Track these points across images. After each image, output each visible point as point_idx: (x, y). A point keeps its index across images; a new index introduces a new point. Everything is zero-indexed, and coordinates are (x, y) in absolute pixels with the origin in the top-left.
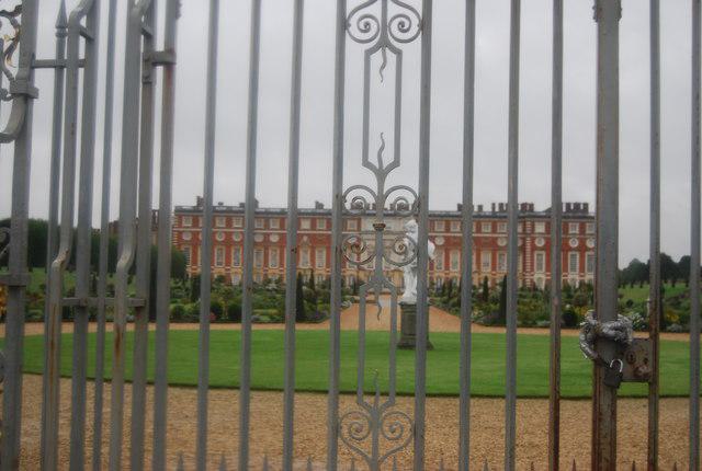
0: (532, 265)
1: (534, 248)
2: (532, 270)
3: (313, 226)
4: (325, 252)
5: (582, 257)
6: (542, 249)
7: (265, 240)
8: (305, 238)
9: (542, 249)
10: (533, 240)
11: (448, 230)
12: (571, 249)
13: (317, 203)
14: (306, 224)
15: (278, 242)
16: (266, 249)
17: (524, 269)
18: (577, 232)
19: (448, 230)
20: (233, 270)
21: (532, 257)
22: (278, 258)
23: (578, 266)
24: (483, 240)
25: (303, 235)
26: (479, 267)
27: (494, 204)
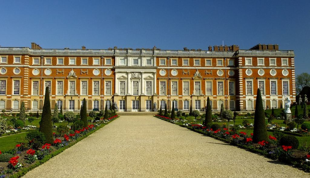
2: (244, 93)
3: (78, 63)
5: (280, 83)
7: (40, 74)
8: (72, 72)
10: (244, 70)
12: (272, 77)
14: (71, 62)
15: (52, 74)
19: (180, 65)
20: (13, 98)
21: (244, 83)
23: (277, 90)
24: (207, 72)
25: (71, 69)
26: (204, 93)
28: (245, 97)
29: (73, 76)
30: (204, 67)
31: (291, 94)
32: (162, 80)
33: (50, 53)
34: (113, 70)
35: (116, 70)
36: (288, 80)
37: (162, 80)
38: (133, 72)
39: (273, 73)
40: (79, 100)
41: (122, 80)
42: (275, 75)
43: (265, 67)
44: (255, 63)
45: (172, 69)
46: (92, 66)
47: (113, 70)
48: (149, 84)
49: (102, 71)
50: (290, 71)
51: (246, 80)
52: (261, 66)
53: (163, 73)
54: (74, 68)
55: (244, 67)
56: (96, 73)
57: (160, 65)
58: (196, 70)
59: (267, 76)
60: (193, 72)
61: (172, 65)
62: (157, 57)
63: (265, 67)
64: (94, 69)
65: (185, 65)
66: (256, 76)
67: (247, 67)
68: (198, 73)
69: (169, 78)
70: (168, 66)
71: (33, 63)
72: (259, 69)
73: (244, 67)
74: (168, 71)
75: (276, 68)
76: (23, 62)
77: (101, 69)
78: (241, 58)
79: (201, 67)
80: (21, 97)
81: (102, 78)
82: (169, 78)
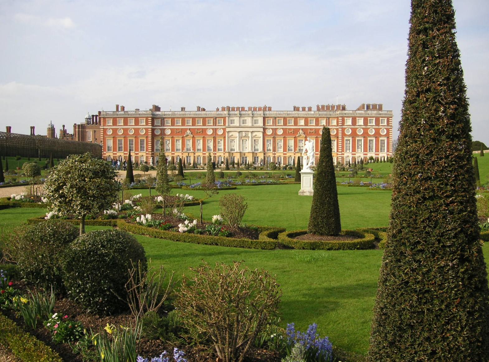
0: (343, 147)
1: (344, 134)
2: (343, 151)
4: (201, 141)
5: (377, 141)
6: (349, 136)
9: (349, 136)
10: (343, 130)
11: (285, 124)
12: (370, 136)
13: (199, 108)
16: (163, 139)
17: (337, 151)
18: (374, 124)
22: (170, 145)
25: (187, 129)
27: (318, 106)
28: (343, 154)
29: (188, 135)
30: (308, 126)
31: (388, 151)
32: (268, 139)
33: (169, 115)
34: (224, 130)
35: (228, 130)
36: (386, 139)
37: (268, 139)
38: (242, 131)
39: (372, 132)
40: (194, 156)
41: (233, 139)
42: (373, 134)
43: (364, 127)
44: (354, 122)
45: (277, 128)
46: (205, 126)
47: (224, 130)
48: (255, 142)
49: (215, 130)
50: (388, 130)
51: (345, 138)
52: (360, 126)
53: (269, 132)
54: (190, 129)
55: (343, 127)
56: (210, 132)
57: (266, 125)
58: (300, 129)
59: (365, 135)
60: (296, 131)
61: (277, 125)
62: (264, 118)
63: (364, 127)
64: (207, 128)
65: (291, 125)
66: (354, 134)
67: (346, 127)
68: (301, 131)
69: (274, 135)
70: (273, 126)
71: (155, 124)
72: (357, 128)
73: (343, 127)
74: (275, 130)
75: (374, 127)
76: (147, 124)
77: (213, 129)
78: (341, 118)
79: (305, 126)
80: (147, 154)
81: (215, 136)
82: (274, 135)
